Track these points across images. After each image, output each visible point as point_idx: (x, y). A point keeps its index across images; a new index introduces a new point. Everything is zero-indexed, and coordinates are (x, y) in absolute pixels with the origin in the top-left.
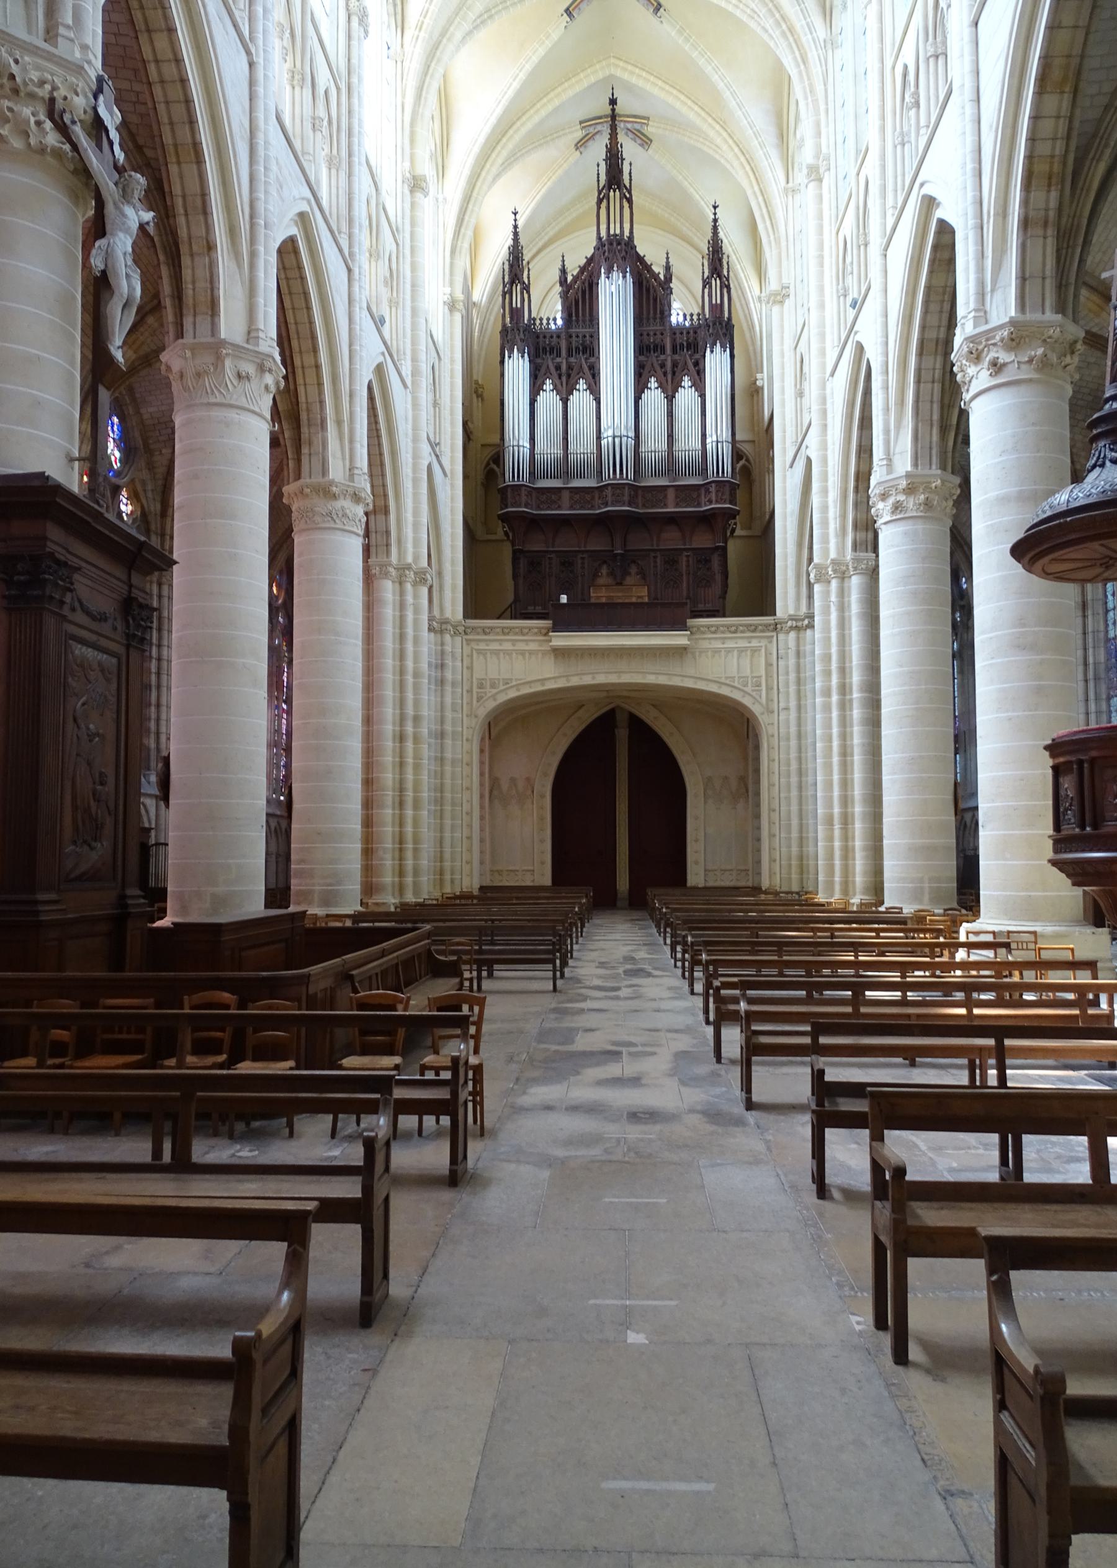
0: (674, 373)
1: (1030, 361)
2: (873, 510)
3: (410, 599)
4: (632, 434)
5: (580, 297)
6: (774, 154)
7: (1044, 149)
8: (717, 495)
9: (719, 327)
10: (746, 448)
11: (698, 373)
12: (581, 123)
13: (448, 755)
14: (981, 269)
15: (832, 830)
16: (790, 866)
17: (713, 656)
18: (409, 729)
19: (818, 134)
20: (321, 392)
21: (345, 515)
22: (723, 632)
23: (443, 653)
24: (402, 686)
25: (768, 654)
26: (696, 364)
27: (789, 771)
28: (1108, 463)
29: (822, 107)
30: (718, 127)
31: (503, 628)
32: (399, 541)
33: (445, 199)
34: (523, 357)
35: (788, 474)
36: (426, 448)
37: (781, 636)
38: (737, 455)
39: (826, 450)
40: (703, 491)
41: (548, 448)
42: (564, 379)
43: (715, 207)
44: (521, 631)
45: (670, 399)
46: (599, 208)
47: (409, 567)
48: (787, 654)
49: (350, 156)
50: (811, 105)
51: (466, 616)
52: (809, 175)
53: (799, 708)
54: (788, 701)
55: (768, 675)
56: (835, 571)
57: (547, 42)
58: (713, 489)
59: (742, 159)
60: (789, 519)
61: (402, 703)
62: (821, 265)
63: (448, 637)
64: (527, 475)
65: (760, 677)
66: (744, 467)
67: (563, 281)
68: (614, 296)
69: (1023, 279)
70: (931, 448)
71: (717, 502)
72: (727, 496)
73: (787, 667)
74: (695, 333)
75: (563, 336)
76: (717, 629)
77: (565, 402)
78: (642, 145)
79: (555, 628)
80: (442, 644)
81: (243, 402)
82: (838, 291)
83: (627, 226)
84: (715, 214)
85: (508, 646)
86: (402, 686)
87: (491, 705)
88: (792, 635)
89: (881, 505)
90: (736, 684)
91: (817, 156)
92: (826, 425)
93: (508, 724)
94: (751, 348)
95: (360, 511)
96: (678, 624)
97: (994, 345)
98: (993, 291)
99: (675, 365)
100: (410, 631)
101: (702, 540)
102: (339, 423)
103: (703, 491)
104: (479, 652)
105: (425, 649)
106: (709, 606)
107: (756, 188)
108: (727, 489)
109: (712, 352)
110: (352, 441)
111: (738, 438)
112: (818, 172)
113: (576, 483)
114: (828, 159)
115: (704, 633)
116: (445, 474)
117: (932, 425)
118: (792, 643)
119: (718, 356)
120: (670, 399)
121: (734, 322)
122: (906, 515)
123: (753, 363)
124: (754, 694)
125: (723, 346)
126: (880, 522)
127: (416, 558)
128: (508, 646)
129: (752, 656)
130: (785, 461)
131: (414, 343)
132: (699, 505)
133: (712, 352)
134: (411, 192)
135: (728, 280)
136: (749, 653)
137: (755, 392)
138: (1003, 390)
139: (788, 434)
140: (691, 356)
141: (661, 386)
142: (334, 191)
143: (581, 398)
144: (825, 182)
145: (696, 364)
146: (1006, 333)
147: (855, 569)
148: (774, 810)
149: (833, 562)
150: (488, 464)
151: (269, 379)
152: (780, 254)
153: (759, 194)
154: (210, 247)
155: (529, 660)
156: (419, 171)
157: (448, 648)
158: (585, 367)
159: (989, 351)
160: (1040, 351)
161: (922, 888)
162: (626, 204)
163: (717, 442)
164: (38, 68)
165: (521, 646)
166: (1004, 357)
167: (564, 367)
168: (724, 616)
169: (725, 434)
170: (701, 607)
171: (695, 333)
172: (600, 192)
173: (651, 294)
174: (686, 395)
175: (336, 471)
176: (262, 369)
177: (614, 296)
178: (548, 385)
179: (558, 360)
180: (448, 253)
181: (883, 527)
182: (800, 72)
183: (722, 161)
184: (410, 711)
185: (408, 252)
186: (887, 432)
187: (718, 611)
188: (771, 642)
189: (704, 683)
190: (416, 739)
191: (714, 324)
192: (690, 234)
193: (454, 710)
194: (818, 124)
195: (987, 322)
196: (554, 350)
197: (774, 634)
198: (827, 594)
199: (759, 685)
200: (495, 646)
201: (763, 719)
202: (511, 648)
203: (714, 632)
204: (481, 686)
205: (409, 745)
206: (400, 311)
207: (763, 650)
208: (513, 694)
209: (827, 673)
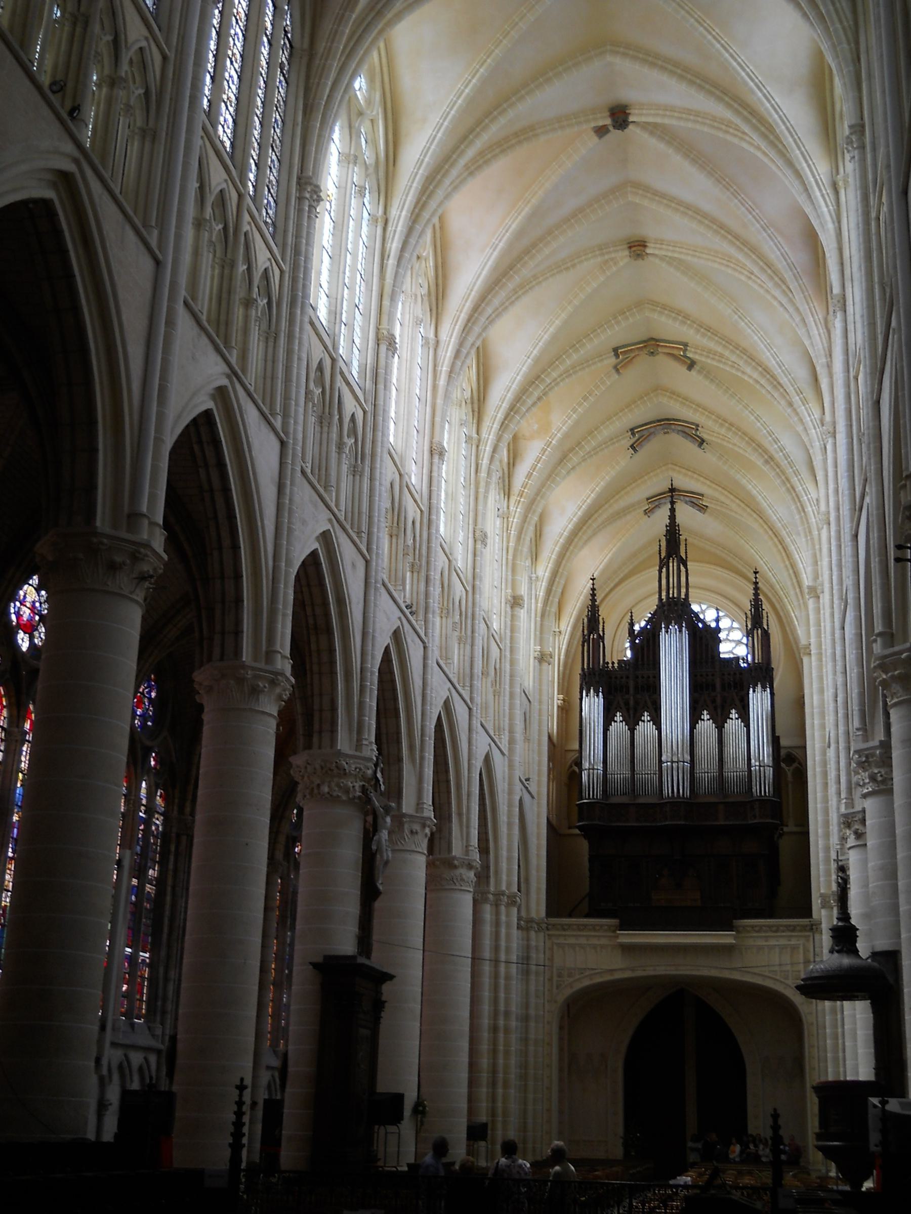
0: (723, 707)
3: (503, 918)
4: (687, 757)
5: (647, 646)
12: (648, 499)
13: (532, 1036)
18: (501, 1022)
20: (449, 797)
21: (462, 880)
22: (766, 932)
23: (528, 947)
24: (495, 988)
25: (806, 951)
31: (578, 925)
32: (497, 872)
33: (537, 577)
34: (598, 696)
36: (518, 786)
41: (619, 771)
42: (631, 712)
43: (756, 573)
44: (594, 928)
45: (720, 727)
46: (660, 572)
47: (503, 894)
49: (473, 632)
50: (810, 542)
51: (549, 914)
61: (495, 1001)
63: (533, 934)
67: (631, 631)
76: (760, 929)
77: (632, 730)
78: (700, 511)
80: (528, 940)
81: (413, 848)
83: (683, 590)
85: (583, 941)
86: (495, 988)
87: (568, 992)
90: (778, 978)
92: (827, 783)
93: (584, 1008)
95: (472, 874)
96: (726, 925)
100: (503, 943)
102: (460, 815)
104: (558, 945)
105: (514, 945)
107: (787, 563)
109: (754, 691)
110: (468, 827)
113: (641, 800)
116: (533, 797)
120: (720, 727)
125: (764, 688)
127: (509, 885)
128: (583, 941)
131: (511, 718)
134: (512, 607)
142: (462, 657)
143: (646, 728)
150: (571, 766)
151: (427, 831)
154: (400, 760)
155: (600, 953)
156: (518, 593)
157: (533, 943)
163: (760, 766)
164: (355, 763)
165: (595, 941)
167: (632, 703)
169: (767, 760)
171: (741, 674)
172: (661, 560)
173: (703, 640)
174: (733, 724)
175: (457, 850)
176: (424, 826)
178: (618, 717)
179: (627, 696)
180: (539, 619)
182: (801, 518)
184: (502, 1008)
185: (508, 654)
188: (808, 941)
190: (507, 1030)
192: (744, 570)
193: (537, 996)
197: (811, 934)
200: (572, 941)
202: (586, 942)
204: (560, 975)
205: (501, 1035)
206: (502, 698)
207: (801, 947)
208: (586, 983)
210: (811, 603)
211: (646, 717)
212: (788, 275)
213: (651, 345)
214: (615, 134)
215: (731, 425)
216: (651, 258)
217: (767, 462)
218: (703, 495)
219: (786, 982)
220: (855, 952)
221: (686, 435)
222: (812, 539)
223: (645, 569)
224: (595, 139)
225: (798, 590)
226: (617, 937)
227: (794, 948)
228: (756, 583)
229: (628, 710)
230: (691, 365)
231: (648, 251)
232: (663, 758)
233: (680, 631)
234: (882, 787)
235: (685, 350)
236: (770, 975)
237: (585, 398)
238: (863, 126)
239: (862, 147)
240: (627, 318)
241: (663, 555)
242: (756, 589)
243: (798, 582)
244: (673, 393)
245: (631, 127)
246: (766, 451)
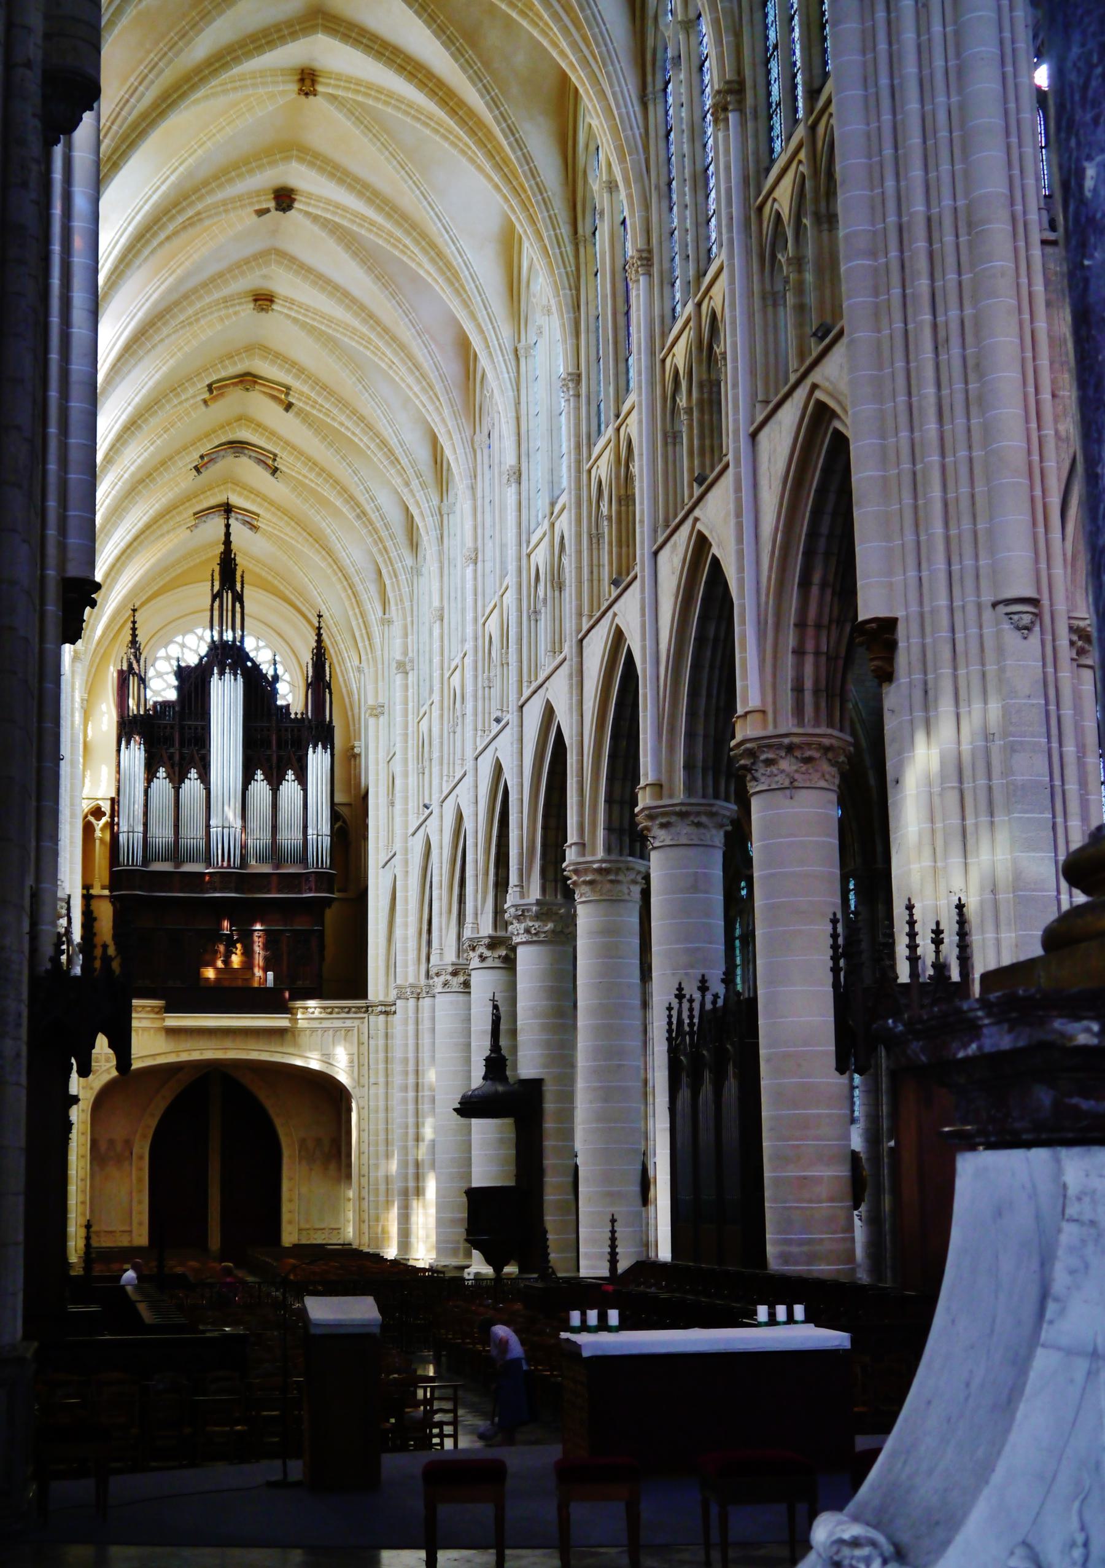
1: (500, 957)
9: (318, 728)
10: (343, 811)
12: (195, 514)
14: (476, 900)
17: (311, 1035)
19: (406, 636)
29: (409, 619)
30: (324, 553)
39: (407, 892)
45: (275, 791)
52: (398, 668)
53: (387, 1083)
54: (377, 1077)
56: (412, 993)
57: (176, 489)
58: (312, 879)
62: (406, 742)
64: (140, 858)
66: (340, 828)
68: (226, 698)
73: (377, 1045)
75: (177, 728)
79: (170, 1008)
88: (382, 1018)
91: (405, 653)
94: (350, 713)
99: (279, 758)
101: (301, 925)
107: (357, 611)
111: (336, 800)
113: (188, 868)
114: (412, 661)
120: (275, 791)
121: (334, 724)
123: (352, 728)
125: (324, 748)
136: (343, 1032)
141: (266, 778)
143: (192, 785)
144: (410, 675)
149: (412, 986)
150: (86, 816)
152: (377, 671)
158: (197, 758)
161: (458, 1248)
162: (238, 605)
166: (487, 953)
167: (177, 758)
173: (258, 688)
174: (290, 787)
177: (226, 698)
178: (162, 772)
186: (441, 930)
191: (317, 728)
192: (293, 597)
194: (405, 628)
196: (168, 741)
198: (406, 1008)
209: (406, 1073)
210: (399, 679)
211: (193, 774)
212: (438, 388)
213: (248, 380)
214: (275, 214)
215: (323, 470)
216: (275, 314)
217: (358, 517)
218: (258, 515)
220: (503, 1079)
221: (260, 461)
222: (403, 609)
223: (178, 587)
224: (254, 217)
225: (367, 643)
226: (163, 1019)
227: (348, 1030)
228: (319, 628)
229: (173, 766)
230: (289, 407)
231: (275, 307)
232: (213, 822)
233: (235, 679)
234: (535, 939)
235: (287, 394)
237: (166, 430)
238: (579, 375)
239: (578, 396)
240: (235, 364)
241: (217, 588)
242: (319, 635)
243: (367, 633)
244: (259, 425)
245: (293, 211)
246: (358, 505)
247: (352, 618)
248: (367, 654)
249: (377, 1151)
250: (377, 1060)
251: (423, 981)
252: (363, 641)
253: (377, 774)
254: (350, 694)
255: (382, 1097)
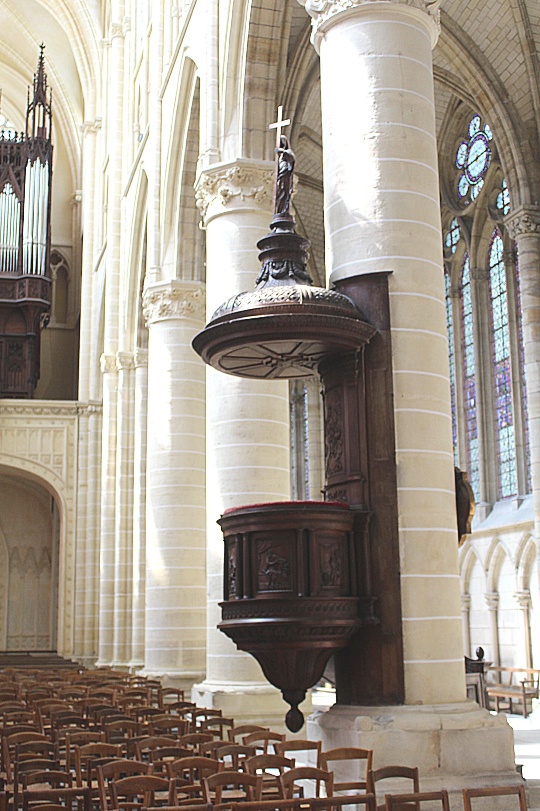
2: (144, 311)
6: (93, 13)
7: (265, 32)
8: (29, 290)
11: (19, 182)
14: (217, 118)
15: (113, 598)
16: (83, 631)
22: (28, 413)
25: (70, 434)
26: (18, 175)
27: (85, 543)
28: (270, 278)
35: (94, 276)
37: (82, 419)
38: (53, 257)
40: (17, 284)
48: (87, 436)
54: (86, 479)
55: (69, 454)
58: (27, 283)
59: (67, 12)
60: (93, 316)
65: (61, 455)
66: (61, 268)
69: (248, 130)
70: (193, 263)
71: (29, 296)
72: (39, 291)
73: (87, 447)
74: (19, 148)
82: (133, 127)
84: (42, 53)
88: (92, 418)
89: (151, 307)
90: (39, 461)
92: (119, 237)
94: (73, 169)
97: (225, 179)
98: (225, 136)
103: (17, 284)
106: (19, 389)
107: (78, 38)
108: (40, 285)
109: (32, 166)
112: (121, 31)
114: (129, 21)
115: (11, 413)
117: (194, 244)
118: (91, 427)
119: (38, 170)
122: (172, 317)
124: (55, 471)
125: (42, 162)
126: (150, 321)
129: (55, 436)
130: (91, 266)
132: (13, 297)
133: (32, 166)
135: (50, 108)
136: (52, 433)
137: (74, 205)
138: (231, 217)
139: (95, 243)
140: (13, 167)
145: (18, 175)
146: (233, 171)
147: (139, 362)
148: (70, 580)
152: (95, 93)
153: (79, 42)
159: (221, 183)
160: (260, 189)
163: (33, 243)
166: (233, 190)
168: (32, 398)
170: (11, 389)
171: (19, 148)
181: (152, 326)
183: (51, 12)
187: (27, 393)
188: (73, 424)
189: (8, 459)
191: (36, 143)
192: (24, 67)
195: (220, 161)
197: (76, 417)
199: (61, 463)
201: (63, 495)
203: (21, 413)
219: (47, 466)
227: (57, 431)
236: (31, 459)
247: (73, 45)
248: (86, 78)
249: (85, 554)
250: (86, 461)
251: (136, 350)
252: (83, 65)
253: (93, 186)
254: (73, 151)
255: (90, 498)
